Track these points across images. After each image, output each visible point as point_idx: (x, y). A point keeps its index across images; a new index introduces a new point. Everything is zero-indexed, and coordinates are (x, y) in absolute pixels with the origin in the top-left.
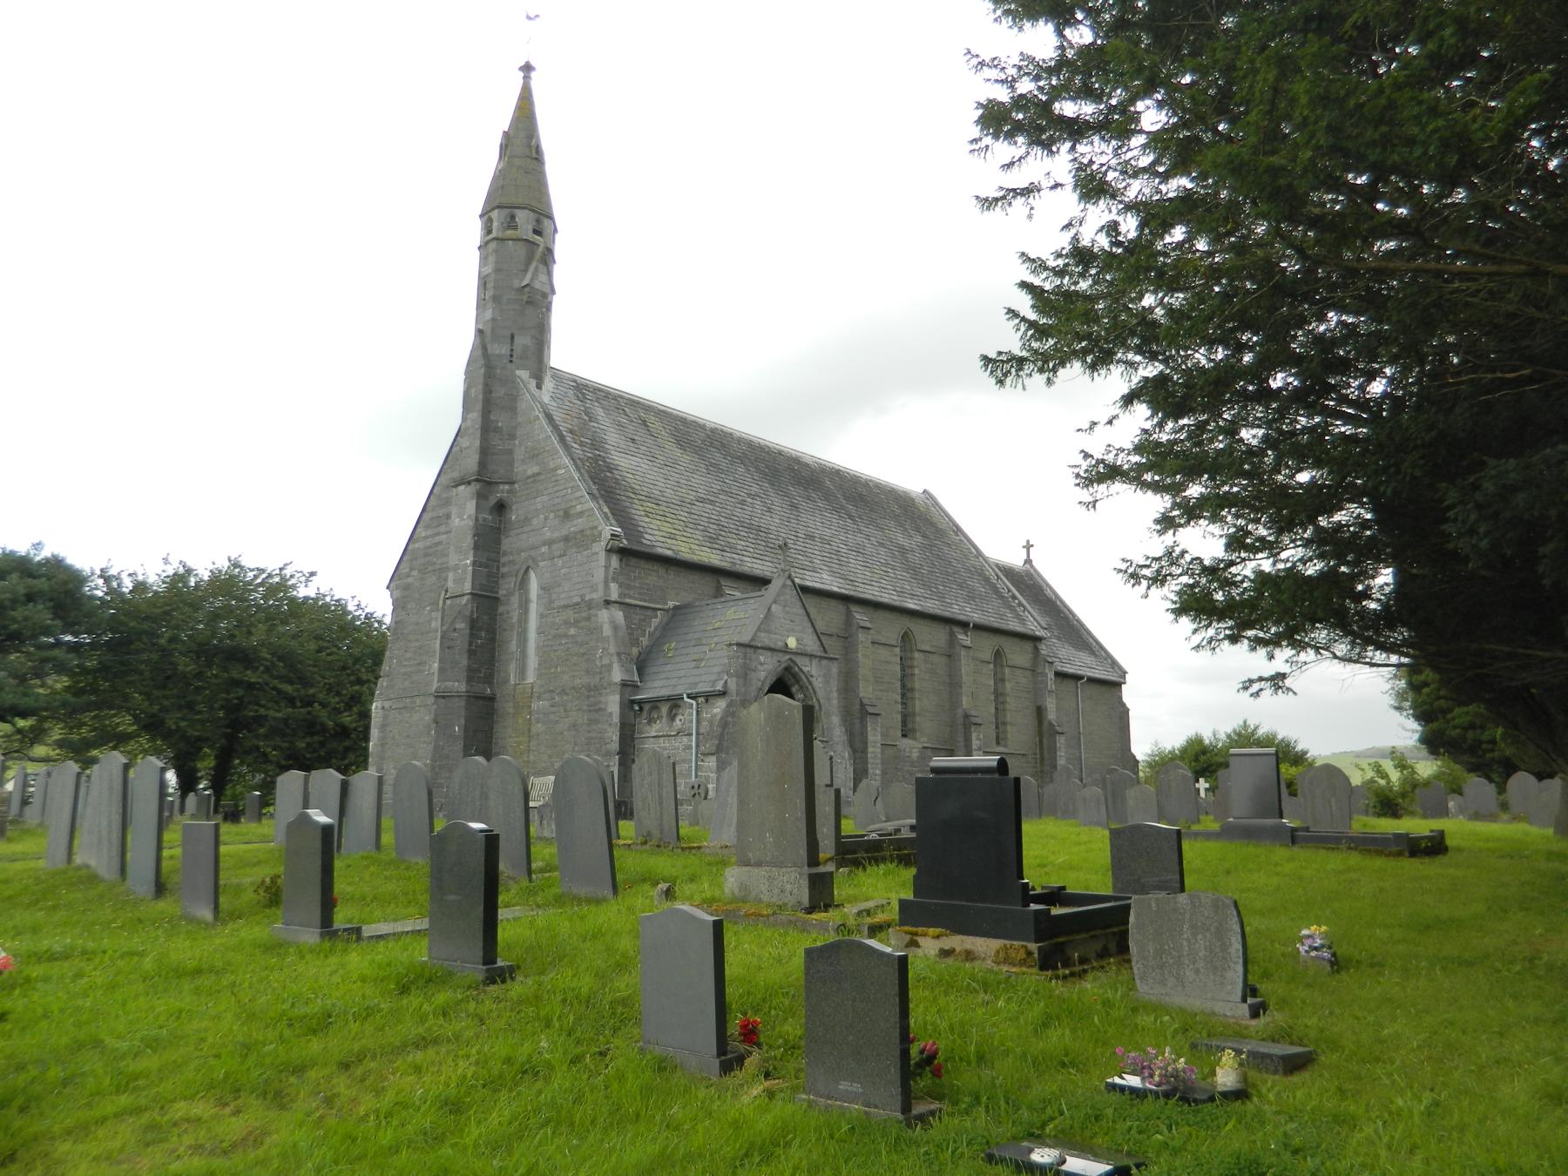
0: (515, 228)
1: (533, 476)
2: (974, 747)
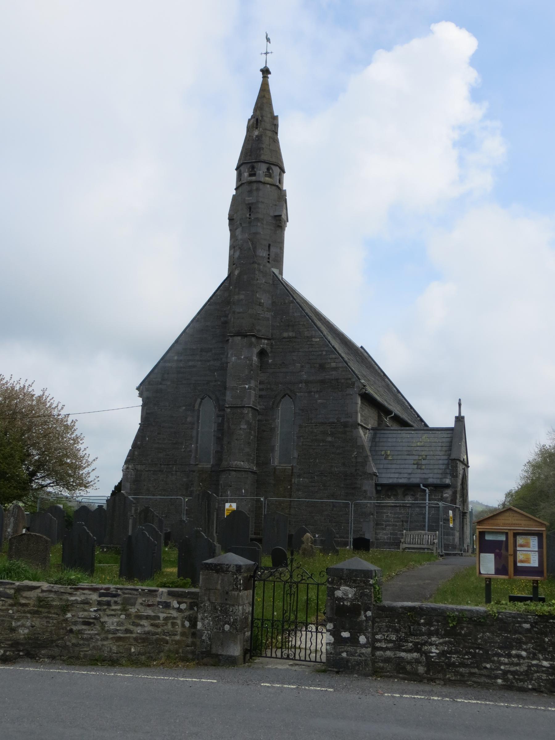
0: (270, 176)
1: (289, 337)
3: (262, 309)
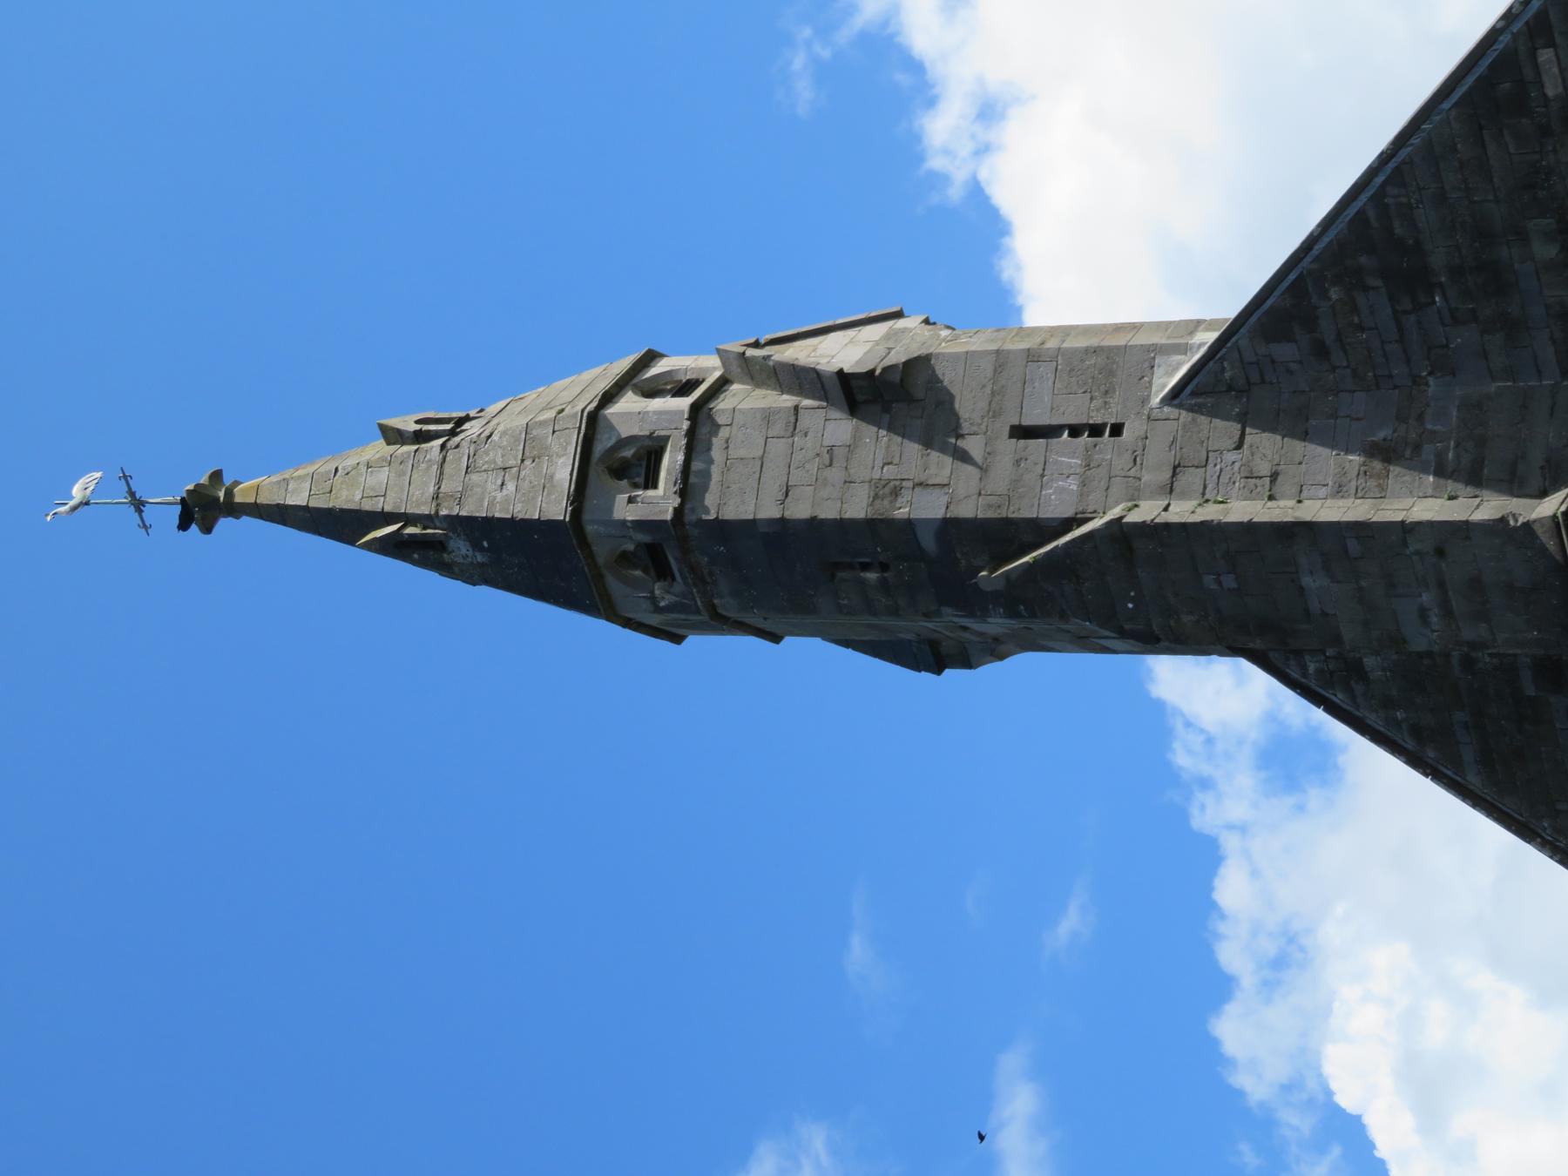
3: (1408, 453)
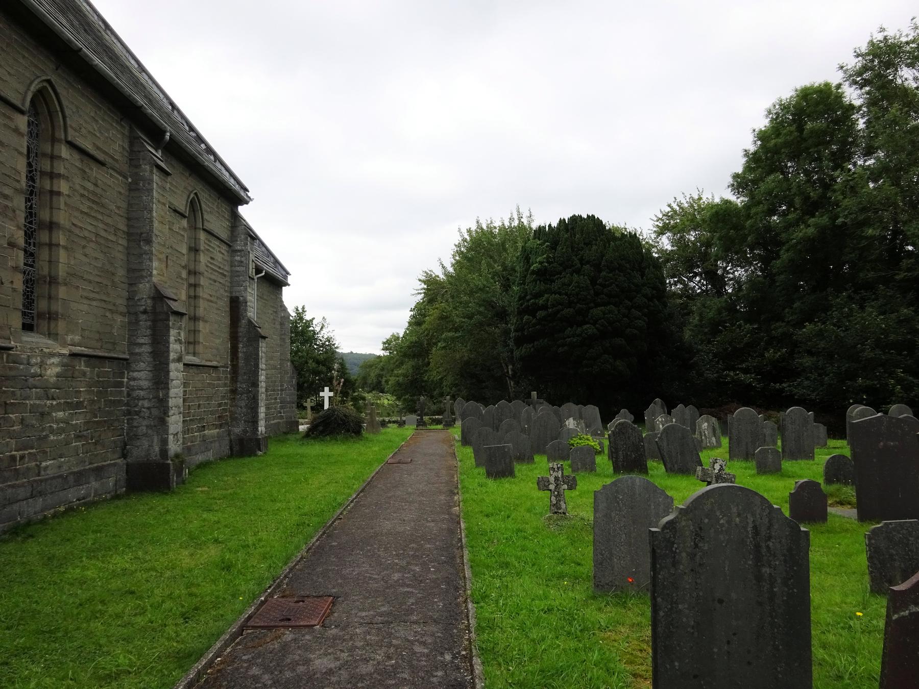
2: (172, 356)
